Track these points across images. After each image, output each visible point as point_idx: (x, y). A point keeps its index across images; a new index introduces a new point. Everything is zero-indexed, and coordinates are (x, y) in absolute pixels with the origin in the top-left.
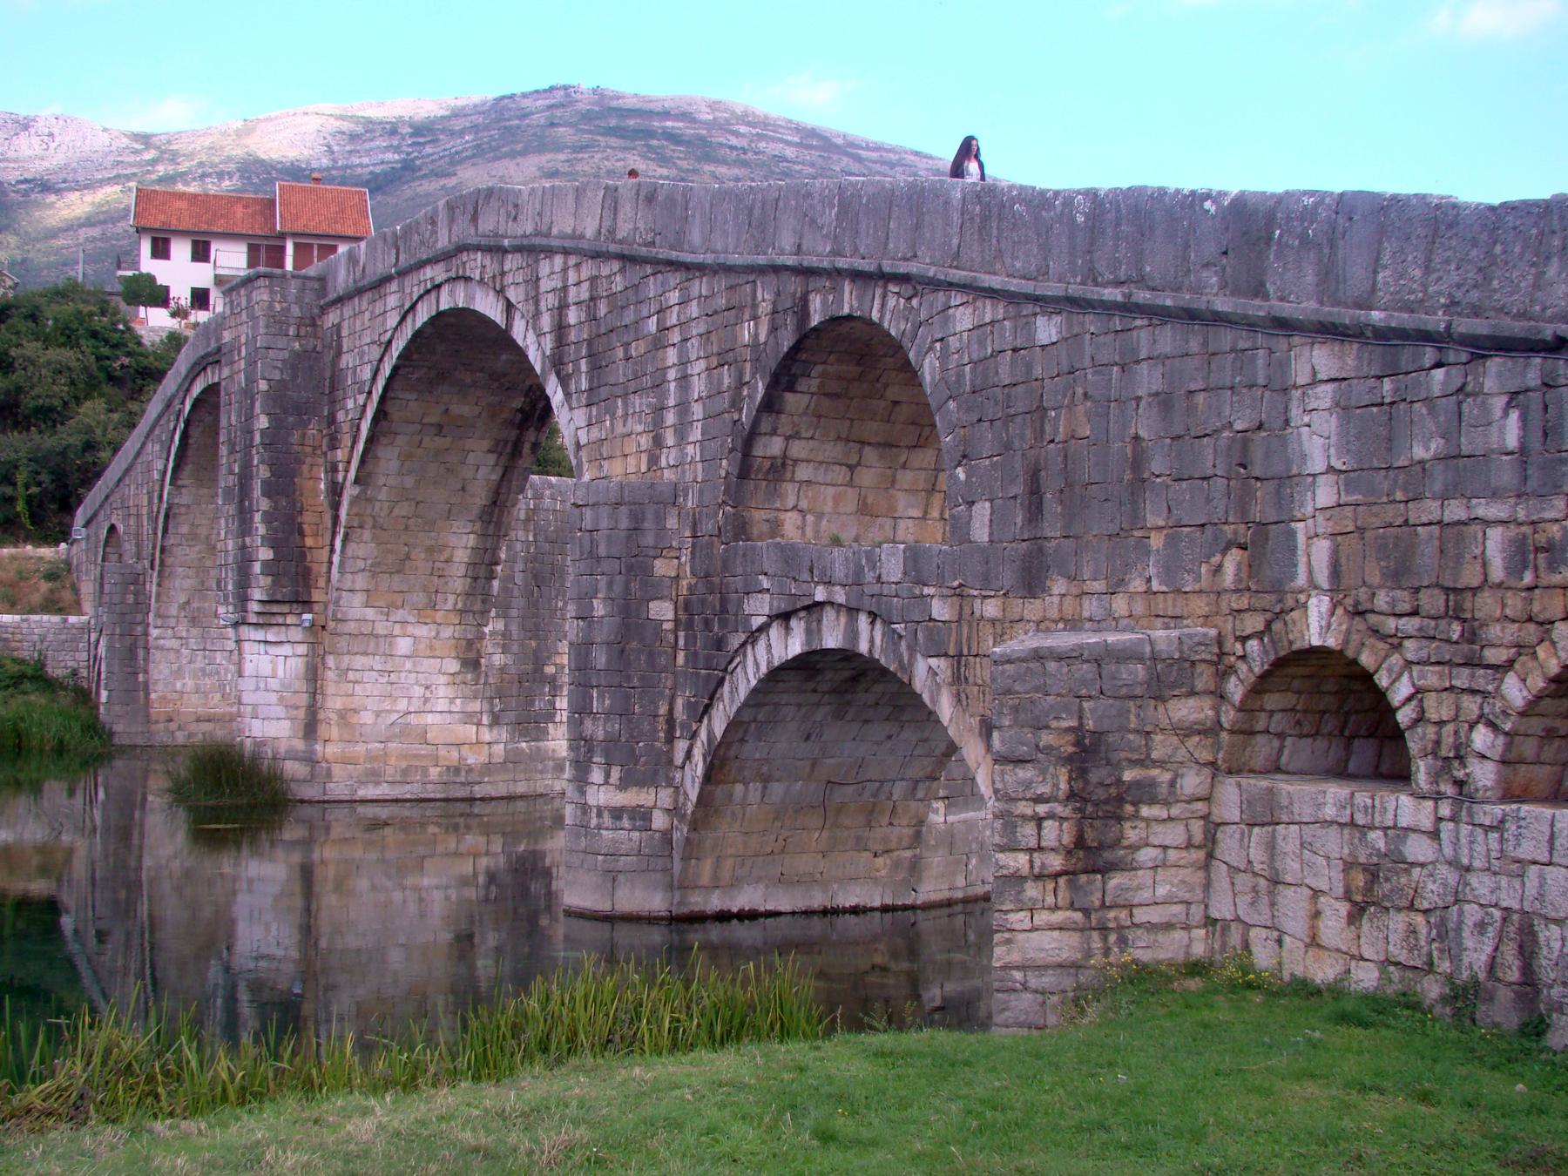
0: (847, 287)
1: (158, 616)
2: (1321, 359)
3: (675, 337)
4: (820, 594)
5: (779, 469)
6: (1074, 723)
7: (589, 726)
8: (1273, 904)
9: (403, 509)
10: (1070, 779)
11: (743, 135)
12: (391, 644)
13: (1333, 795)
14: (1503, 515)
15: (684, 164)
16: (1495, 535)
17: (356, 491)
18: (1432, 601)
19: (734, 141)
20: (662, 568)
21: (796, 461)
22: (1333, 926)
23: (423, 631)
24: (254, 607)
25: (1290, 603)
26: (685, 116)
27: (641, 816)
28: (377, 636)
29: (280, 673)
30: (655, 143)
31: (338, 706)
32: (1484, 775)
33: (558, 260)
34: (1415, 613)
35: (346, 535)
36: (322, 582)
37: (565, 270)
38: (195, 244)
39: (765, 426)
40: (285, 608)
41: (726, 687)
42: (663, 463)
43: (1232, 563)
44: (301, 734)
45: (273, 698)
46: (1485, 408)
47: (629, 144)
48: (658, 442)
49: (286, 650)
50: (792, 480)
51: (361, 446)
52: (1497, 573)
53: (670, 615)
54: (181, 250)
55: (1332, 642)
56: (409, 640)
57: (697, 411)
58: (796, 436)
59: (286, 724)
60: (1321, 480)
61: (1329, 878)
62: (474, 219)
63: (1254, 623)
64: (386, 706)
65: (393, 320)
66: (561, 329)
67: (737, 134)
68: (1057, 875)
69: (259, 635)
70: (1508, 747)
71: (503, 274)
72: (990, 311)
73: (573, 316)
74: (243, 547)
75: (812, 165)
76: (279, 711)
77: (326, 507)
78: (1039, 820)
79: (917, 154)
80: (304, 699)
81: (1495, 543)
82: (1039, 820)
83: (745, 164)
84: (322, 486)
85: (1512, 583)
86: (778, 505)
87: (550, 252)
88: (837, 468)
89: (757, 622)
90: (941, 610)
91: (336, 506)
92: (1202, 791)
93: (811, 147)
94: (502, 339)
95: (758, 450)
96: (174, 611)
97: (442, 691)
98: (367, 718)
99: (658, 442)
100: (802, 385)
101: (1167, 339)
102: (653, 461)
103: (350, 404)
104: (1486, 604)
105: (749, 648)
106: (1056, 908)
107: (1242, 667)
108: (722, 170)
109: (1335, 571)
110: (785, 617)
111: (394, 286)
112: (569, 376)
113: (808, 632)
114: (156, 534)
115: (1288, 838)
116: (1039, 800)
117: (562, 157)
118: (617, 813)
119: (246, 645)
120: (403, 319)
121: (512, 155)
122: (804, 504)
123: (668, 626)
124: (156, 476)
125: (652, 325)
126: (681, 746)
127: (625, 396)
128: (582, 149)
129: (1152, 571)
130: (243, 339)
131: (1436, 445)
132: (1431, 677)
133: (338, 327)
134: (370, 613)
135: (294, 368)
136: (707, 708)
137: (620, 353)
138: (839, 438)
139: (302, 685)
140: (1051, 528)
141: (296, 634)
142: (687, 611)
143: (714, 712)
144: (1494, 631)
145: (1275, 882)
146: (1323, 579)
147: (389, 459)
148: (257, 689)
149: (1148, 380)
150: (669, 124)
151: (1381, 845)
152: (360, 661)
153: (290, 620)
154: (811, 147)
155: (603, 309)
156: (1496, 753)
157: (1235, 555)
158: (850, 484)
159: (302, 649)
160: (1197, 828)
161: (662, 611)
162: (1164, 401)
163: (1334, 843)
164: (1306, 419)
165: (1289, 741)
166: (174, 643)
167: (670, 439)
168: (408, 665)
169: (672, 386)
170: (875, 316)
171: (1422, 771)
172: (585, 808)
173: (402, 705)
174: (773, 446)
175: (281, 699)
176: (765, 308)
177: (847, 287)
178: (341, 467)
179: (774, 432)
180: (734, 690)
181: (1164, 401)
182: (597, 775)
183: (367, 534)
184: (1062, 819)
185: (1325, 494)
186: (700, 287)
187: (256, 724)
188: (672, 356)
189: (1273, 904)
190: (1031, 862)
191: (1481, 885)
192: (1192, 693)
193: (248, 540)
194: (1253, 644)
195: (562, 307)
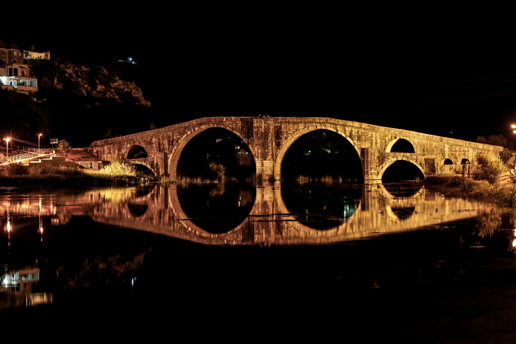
2: (447, 145)
3: (375, 137)
4: (399, 156)
7: (371, 166)
13: (448, 165)
18: (454, 156)
20: (376, 154)
22: (449, 171)
27: (375, 173)
33: (350, 128)
37: (352, 129)
41: (385, 163)
42: (373, 146)
45: (269, 169)
48: (372, 145)
49: (271, 163)
52: (458, 155)
55: (448, 158)
57: (380, 143)
59: (271, 172)
69: (268, 161)
72: (419, 140)
73: (353, 133)
80: (272, 169)
81: (457, 154)
84: (274, 144)
87: (349, 127)
90: (414, 157)
96: (172, 160)
101: (435, 143)
102: (371, 146)
103: (285, 135)
104: (457, 157)
105: (388, 160)
109: (448, 155)
110: (393, 158)
112: (353, 138)
113: (397, 159)
115: (445, 167)
118: (374, 173)
119: (264, 163)
125: (370, 136)
127: (365, 141)
130: (263, 126)
131: (454, 150)
132: (454, 160)
133: (280, 126)
137: (364, 137)
139: (272, 167)
140: (426, 153)
141: (272, 161)
142: (378, 157)
143: (383, 165)
146: (447, 155)
149: (434, 145)
155: (360, 133)
159: (273, 163)
161: (376, 158)
162: (435, 147)
163: (449, 167)
166: (171, 165)
167: (374, 144)
169: (374, 141)
170: (405, 139)
171: (454, 164)
172: (371, 173)
175: (270, 169)
181: (435, 147)
182: (372, 170)
185: (447, 151)
186: (378, 134)
191: (457, 168)
193: (266, 151)
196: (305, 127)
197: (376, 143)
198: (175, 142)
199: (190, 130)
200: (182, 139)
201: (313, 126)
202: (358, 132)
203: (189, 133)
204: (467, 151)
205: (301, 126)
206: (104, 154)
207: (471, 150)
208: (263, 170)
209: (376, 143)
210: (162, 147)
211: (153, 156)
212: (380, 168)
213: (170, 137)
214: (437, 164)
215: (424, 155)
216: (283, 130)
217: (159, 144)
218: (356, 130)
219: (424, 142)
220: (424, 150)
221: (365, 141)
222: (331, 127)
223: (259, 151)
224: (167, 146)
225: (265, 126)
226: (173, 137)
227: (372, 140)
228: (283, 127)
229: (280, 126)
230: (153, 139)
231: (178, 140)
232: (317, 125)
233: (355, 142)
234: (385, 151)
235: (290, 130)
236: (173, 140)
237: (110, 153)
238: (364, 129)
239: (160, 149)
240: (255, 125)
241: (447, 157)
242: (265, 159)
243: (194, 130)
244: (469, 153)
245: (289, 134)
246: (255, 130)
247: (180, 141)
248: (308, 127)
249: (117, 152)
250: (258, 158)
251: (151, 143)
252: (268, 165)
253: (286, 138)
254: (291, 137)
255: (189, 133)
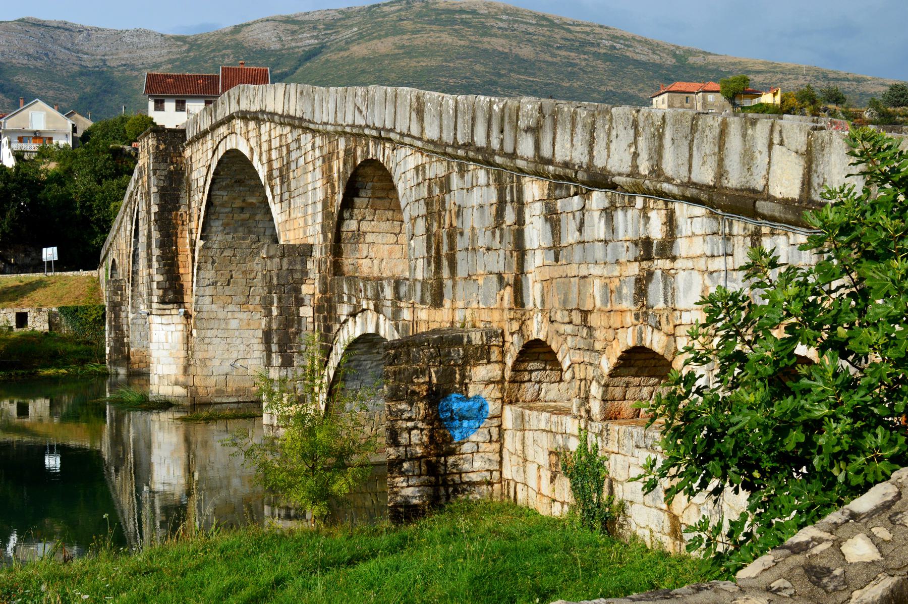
0: (371, 144)
1: (132, 307)
5: (359, 235)
6: (427, 379)
8: (525, 472)
9: (228, 253)
10: (425, 409)
11: (505, 21)
12: (227, 323)
14: (600, 273)
15: (473, 38)
16: (598, 283)
17: (202, 242)
18: (577, 318)
19: (501, 25)
21: (365, 233)
23: (245, 316)
24: (155, 306)
25: (528, 316)
26: (474, 12)
28: (219, 319)
29: (170, 341)
30: (457, 27)
31: (200, 357)
32: (596, 407)
34: (570, 322)
35: (199, 269)
36: (189, 292)
38: (177, 102)
39: (346, 215)
40: (171, 306)
44: (181, 371)
46: (592, 217)
47: (442, 28)
49: (172, 327)
50: (364, 242)
51: (201, 220)
52: (598, 304)
53: (311, 314)
54: (170, 105)
55: (542, 337)
56: (237, 321)
58: (364, 219)
60: (537, 252)
61: (543, 459)
62: (238, 102)
63: (515, 326)
64: (226, 356)
65: (210, 154)
66: (270, 161)
67: (502, 20)
68: (419, 459)
70: (605, 393)
71: (248, 132)
73: (274, 155)
74: (150, 274)
75: (544, 36)
76: (171, 360)
77: (189, 253)
78: (409, 430)
79: (601, 27)
80: (183, 354)
81: (596, 288)
82: (409, 430)
83: (507, 37)
85: (604, 308)
86: (358, 256)
88: (389, 235)
89: (343, 318)
91: (193, 251)
92: (497, 413)
93: (542, 26)
94: (248, 164)
95: (344, 229)
97: (256, 347)
98: (216, 362)
100: (362, 193)
103: (196, 197)
106: (420, 475)
107: (512, 348)
108: (494, 40)
110: (353, 315)
111: (209, 137)
113: (363, 324)
116: (410, 419)
117: (406, 37)
119: (153, 326)
120: (214, 153)
121: (379, 37)
122: (371, 255)
123: (310, 320)
124: (128, 234)
126: (318, 382)
128: (418, 32)
129: (479, 297)
134: (214, 307)
135: (170, 179)
136: (327, 363)
138: (388, 220)
139: (181, 346)
144: (597, 334)
145: (526, 460)
147: (216, 225)
148: (159, 348)
150: (464, 16)
151: (561, 442)
152: (209, 333)
153: (174, 312)
154: (542, 26)
156: (599, 396)
157: (508, 288)
158: (397, 243)
159: (181, 327)
160: (495, 431)
163: (546, 442)
164: (531, 219)
165: (544, 386)
168: (237, 333)
173: (235, 355)
174: (351, 225)
175: (171, 354)
176: (342, 154)
177: (371, 144)
178: (194, 231)
179: (351, 218)
180: (336, 354)
183: (209, 266)
184: (422, 430)
187: (159, 367)
189: (525, 472)
190: (406, 451)
192: (489, 362)
194: (515, 336)
195: (270, 149)
241: (537, 329)
244: (681, 277)
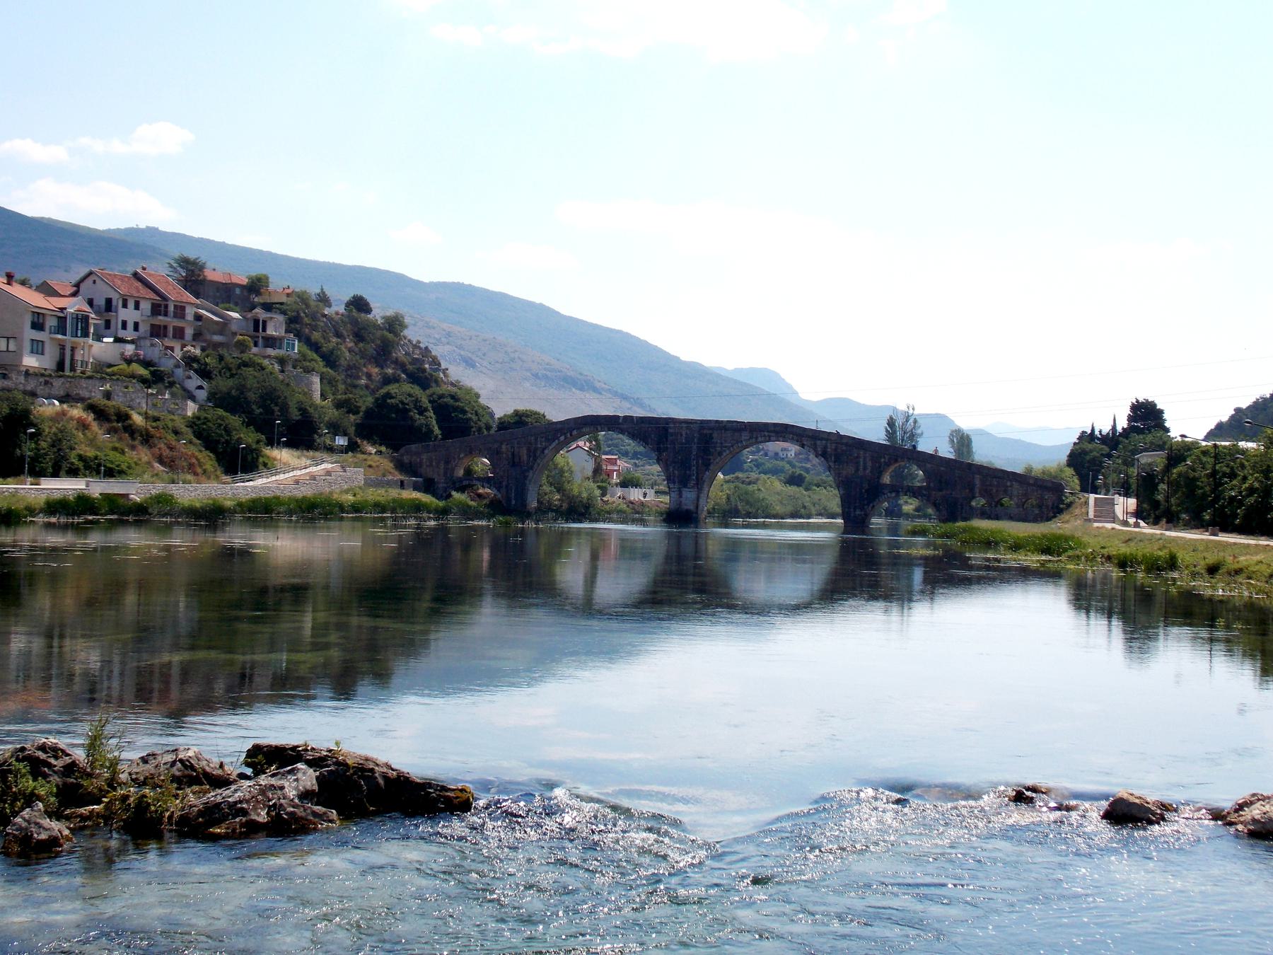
43: (967, 491)
48: (857, 470)
80: (695, 502)
81: (994, 491)
87: (822, 439)
90: (924, 492)
99: (857, 470)
103: (719, 449)
114: (535, 460)
119: (684, 492)
126: (866, 507)
130: (684, 433)
133: (711, 434)
142: (866, 491)
155: (839, 450)
188: (861, 460)
193: (688, 472)
196: (751, 438)
197: (865, 469)
198: (539, 452)
199: (565, 434)
200: (551, 448)
201: (765, 436)
202: (836, 450)
203: (562, 438)
204: (1010, 486)
205: (745, 435)
206: (421, 467)
207: (1016, 485)
208: (681, 502)
209: (865, 469)
210: (517, 460)
211: (502, 473)
212: (870, 508)
213: (530, 444)
214: (962, 505)
215: (940, 490)
216: (714, 440)
217: (513, 454)
218: (834, 446)
219: (942, 469)
220: (940, 482)
221: (847, 463)
222: (793, 438)
223: (676, 472)
224: (525, 458)
225: (686, 434)
226: (536, 444)
227: (858, 463)
228: (715, 435)
229: (711, 434)
230: (504, 447)
231: (544, 449)
232: (773, 434)
233: (832, 464)
234: (878, 482)
235: (725, 441)
236: (536, 449)
237: (431, 465)
238: (846, 445)
239: (514, 462)
240: (670, 431)
242: (685, 486)
243: (571, 435)
245: (726, 447)
246: (670, 438)
247: (546, 451)
248: (757, 438)
249: (442, 466)
250: (674, 483)
251: (498, 452)
252: (689, 496)
253: (720, 454)
254: (728, 452)
255: (562, 438)
